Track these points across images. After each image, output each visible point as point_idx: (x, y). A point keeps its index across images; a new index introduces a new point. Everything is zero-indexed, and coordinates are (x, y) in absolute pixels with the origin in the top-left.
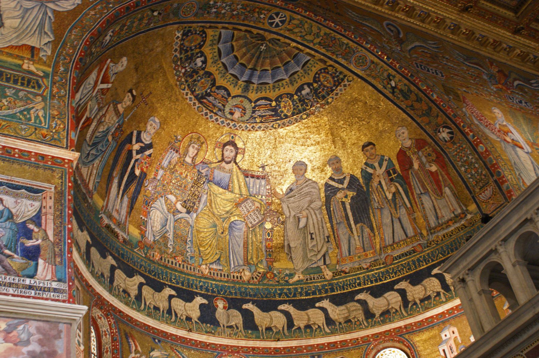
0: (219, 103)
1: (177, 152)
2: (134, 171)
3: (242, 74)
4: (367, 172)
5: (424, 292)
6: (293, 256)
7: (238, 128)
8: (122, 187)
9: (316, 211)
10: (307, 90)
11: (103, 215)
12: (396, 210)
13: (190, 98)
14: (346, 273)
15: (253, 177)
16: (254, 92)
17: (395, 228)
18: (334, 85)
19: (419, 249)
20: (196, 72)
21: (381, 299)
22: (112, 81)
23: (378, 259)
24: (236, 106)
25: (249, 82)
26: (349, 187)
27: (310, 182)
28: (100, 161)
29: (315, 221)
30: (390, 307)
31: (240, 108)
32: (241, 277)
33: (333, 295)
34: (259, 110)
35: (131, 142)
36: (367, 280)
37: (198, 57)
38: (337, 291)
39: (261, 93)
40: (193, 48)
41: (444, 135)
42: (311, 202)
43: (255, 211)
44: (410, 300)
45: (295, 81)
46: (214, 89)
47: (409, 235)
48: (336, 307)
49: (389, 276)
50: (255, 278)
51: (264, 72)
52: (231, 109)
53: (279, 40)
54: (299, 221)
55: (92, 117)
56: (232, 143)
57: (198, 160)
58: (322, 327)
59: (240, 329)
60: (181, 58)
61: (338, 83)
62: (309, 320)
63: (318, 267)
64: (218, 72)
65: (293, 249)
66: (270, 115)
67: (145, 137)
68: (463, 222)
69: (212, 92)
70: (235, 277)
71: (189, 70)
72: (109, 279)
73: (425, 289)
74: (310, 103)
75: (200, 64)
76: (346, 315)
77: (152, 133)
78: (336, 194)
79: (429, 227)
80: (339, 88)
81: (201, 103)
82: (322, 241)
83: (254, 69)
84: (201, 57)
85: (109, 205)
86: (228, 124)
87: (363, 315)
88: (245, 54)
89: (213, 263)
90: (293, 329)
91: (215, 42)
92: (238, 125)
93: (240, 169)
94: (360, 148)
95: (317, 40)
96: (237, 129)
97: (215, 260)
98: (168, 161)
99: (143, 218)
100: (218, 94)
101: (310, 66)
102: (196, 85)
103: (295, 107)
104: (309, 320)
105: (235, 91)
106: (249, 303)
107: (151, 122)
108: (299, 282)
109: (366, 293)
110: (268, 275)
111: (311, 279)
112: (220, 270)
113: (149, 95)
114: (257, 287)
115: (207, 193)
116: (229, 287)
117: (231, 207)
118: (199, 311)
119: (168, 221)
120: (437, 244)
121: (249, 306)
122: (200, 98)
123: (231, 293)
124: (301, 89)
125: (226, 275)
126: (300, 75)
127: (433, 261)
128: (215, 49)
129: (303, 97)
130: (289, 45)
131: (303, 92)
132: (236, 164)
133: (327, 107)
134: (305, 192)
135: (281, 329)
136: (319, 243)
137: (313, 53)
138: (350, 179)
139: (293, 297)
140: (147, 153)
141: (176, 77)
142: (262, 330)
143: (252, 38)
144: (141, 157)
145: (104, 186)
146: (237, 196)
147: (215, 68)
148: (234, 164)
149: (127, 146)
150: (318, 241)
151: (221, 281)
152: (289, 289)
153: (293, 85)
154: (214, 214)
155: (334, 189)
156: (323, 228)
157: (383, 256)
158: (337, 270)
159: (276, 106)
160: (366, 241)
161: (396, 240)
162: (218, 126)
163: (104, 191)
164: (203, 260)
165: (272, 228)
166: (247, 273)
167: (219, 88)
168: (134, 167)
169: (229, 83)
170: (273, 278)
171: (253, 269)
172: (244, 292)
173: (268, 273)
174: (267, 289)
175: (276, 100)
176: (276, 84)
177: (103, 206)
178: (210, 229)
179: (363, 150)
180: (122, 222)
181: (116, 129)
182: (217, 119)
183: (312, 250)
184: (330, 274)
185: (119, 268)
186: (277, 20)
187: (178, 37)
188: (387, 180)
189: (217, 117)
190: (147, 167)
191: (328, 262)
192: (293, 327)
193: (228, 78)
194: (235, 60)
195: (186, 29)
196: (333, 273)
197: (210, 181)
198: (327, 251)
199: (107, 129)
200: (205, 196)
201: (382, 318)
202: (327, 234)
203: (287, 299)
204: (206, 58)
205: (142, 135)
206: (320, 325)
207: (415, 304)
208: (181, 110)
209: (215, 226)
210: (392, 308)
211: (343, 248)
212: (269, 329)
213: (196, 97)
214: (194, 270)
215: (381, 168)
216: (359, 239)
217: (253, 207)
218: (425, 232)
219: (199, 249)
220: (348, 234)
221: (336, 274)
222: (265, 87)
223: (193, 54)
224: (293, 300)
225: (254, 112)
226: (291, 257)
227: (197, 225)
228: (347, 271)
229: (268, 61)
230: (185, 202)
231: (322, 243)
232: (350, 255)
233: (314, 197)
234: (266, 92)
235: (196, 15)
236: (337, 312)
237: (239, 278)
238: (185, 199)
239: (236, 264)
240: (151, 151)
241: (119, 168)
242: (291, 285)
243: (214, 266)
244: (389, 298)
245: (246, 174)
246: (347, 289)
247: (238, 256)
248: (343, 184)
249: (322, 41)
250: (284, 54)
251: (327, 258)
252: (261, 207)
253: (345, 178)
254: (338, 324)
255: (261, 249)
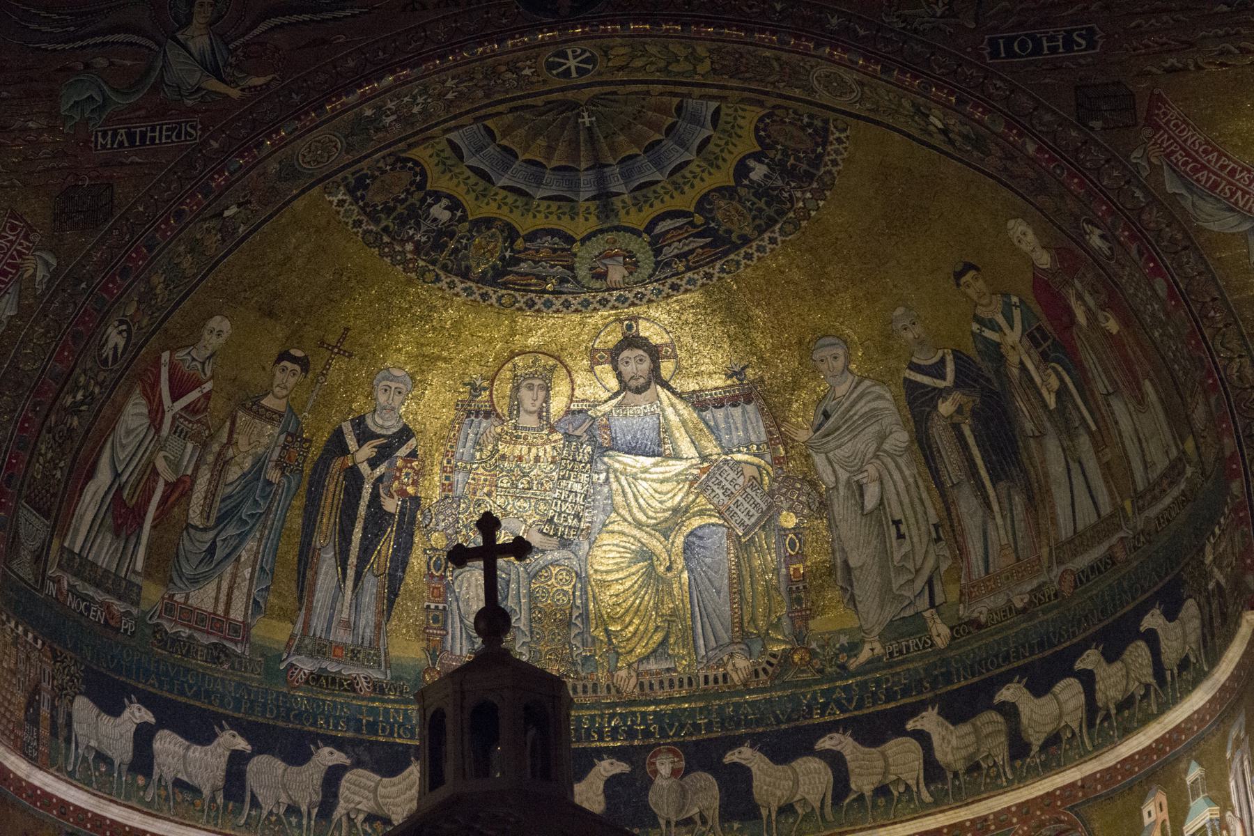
0: (552, 266)
1: (487, 415)
2: (380, 507)
3: (574, 186)
4: (985, 338)
5: (1124, 682)
6: (857, 592)
7: (637, 302)
8: (353, 560)
9: (898, 459)
10: (759, 172)
11: (293, 660)
12: (1072, 441)
13: (465, 290)
14: (980, 626)
15: (719, 404)
16: (633, 210)
17: (1075, 492)
18: (817, 145)
19: (1120, 555)
20: (446, 232)
21: (1049, 697)
22: (209, 374)
23: (1045, 583)
24: (604, 256)
25: (604, 197)
26: (957, 385)
27: (867, 383)
28: (260, 540)
29: (901, 486)
30: (1063, 724)
31: (617, 255)
32: (725, 676)
33: (949, 693)
34: (669, 245)
35: (344, 451)
36: (1024, 647)
37: (430, 205)
38: (959, 681)
39: (651, 206)
40: (403, 196)
41: (1095, 240)
42: (882, 437)
43: (748, 490)
44: (1100, 704)
45: (716, 158)
46: (520, 243)
47: (1103, 514)
48: (952, 728)
49: (1067, 631)
50: (761, 673)
51: (630, 162)
52: (592, 269)
53: (615, 93)
54: (862, 496)
55: (189, 472)
56: (631, 341)
57: (558, 405)
58: (915, 789)
59: (710, 823)
60: (386, 229)
61: (822, 136)
62: (886, 772)
63: (918, 615)
64: (505, 209)
65: (857, 573)
66: (702, 247)
67: (380, 422)
68: (1183, 487)
69: (519, 252)
70: (711, 679)
71: (424, 239)
72: (316, 810)
73: (1128, 673)
74: (786, 195)
75: (446, 215)
76: (971, 750)
77: (396, 404)
78: (935, 407)
79: (1135, 490)
80: (829, 148)
81: (505, 286)
82: (925, 540)
83: (599, 166)
84: (437, 200)
85: (315, 621)
86: (604, 303)
87: (1006, 748)
88: (550, 150)
89: (647, 658)
90: (847, 801)
91: (449, 162)
92: (631, 296)
93: (679, 396)
94: (952, 281)
95: (705, 67)
96: (633, 304)
97: (652, 646)
98: (469, 444)
99: (433, 606)
100: (537, 251)
101: (730, 119)
102: (466, 257)
103: (754, 213)
104: (886, 772)
105: (580, 228)
106: (742, 745)
107: (384, 383)
108: (874, 663)
109: (1019, 682)
110: (796, 658)
111: (900, 652)
112: (668, 670)
113: (344, 337)
114: (767, 695)
115: (607, 479)
116: (693, 710)
117: (680, 495)
118: (601, 798)
119: (513, 586)
120: (1150, 542)
121: (744, 755)
122: (496, 277)
123: (697, 727)
124: (742, 170)
125: (686, 681)
126: (722, 143)
127: (1144, 592)
128: (462, 173)
129: (760, 186)
130: (648, 93)
131: (753, 176)
132: (665, 385)
133: (828, 193)
134: (863, 411)
135: (817, 805)
136: (917, 546)
137: (714, 91)
138: (956, 364)
139: (858, 708)
140: (404, 451)
141: (400, 268)
142: (769, 815)
143: (541, 115)
144: (388, 468)
145: (288, 586)
146: (694, 461)
147: (494, 205)
148: (659, 388)
149: (337, 464)
150: (916, 539)
151: (670, 700)
152: (846, 689)
153: (718, 167)
154: (639, 525)
155: (928, 393)
156: (921, 500)
157: (1056, 571)
158: (959, 619)
159: (707, 223)
160: (1021, 526)
161: (1080, 527)
162: (576, 318)
163: (290, 602)
164: (618, 654)
165: (797, 526)
166: (742, 663)
167: (532, 236)
168: (375, 497)
169: (553, 218)
170: (809, 662)
171: (757, 647)
172: (731, 718)
173: (794, 650)
174: (791, 698)
175: (700, 207)
176: (677, 177)
177: (292, 637)
178: (633, 569)
179: (958, 285)
180: (366, 644)
181: (284, 447)
182: (566, 300)
183: (901, 569)
184: (945, 631)
185: (358, 764)
186: (572, 63)
187: (341, 203)
188: (1036, 356)
189: (564, 297)
190: (415, 483)
191: (938, 601)
192: (847, 796)
193: (542, 208)
194: (534, 168)
195: (351, 180)
196: (952, 629)
197: (601, 450)
198: (937, 568)
199: (253, 466)
200: (606, 489)
201: (1043, 757)
202: (933, 519)
203: (842, 717)
204: (449, 197)
205: (369, 422)
206: (910, 782)
207: (1107, 717)
208: (455, 324)
209: (645, 555)
210: (1067, 726)
211: (973, 556)
212: (787, 810)
213: (482, 280)
214: (595, 691)
215: (1012, 328)
216: (1005, 525)
217: (741, 481)
218: (1128, 504)
219: (606, 631)
220: (980, 513)
221: (958, 632)
222: (655, 192)
223: (413, 204)
224: (855, 718)
225: (657, 252)
226: (852, 595)
227: (596, 567)
228: (983, 619)
229: (622, 138)
230: (551, 521)
231: (924, 546)
232: (987, 572)
233: (886, 422)
234: (662, 201)
235: (349, 148)
236: (954, 742)
237: (720, 680)
238: (551, 513)
239: (713, 643)
240: (413, 442)
241: (328, 521)
242: (853, 675)
243: (653, 666)
244: (1062, 697)
245: (698, 402)
246: (981, 673)
247: (716, 621)
248: (944, 379)
249: (717, 66)
250: (650, 113)
251: (938, 588)
252: (761, 474)
253: (942, 361)
254: (950, 776)
255: (777, 589)
